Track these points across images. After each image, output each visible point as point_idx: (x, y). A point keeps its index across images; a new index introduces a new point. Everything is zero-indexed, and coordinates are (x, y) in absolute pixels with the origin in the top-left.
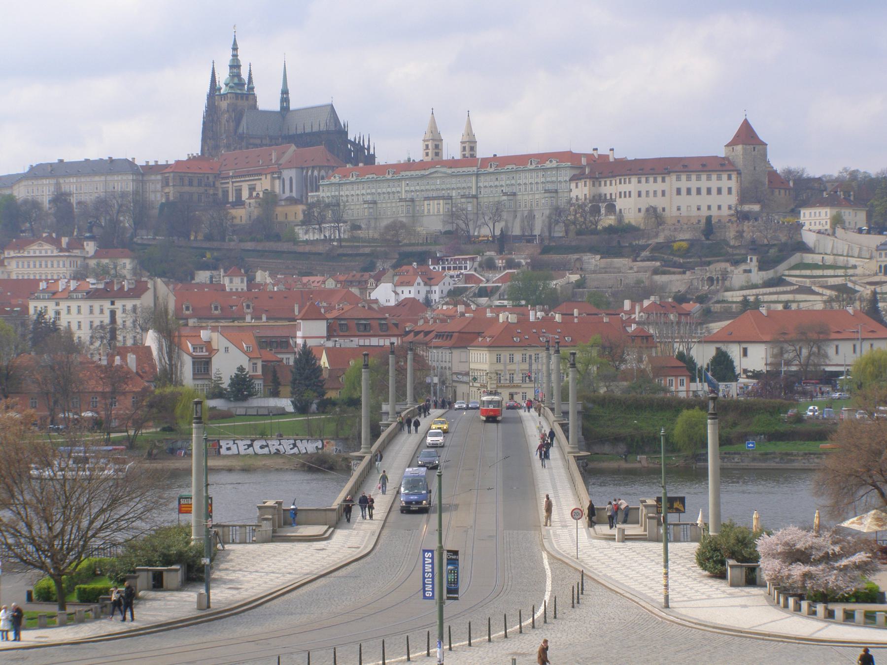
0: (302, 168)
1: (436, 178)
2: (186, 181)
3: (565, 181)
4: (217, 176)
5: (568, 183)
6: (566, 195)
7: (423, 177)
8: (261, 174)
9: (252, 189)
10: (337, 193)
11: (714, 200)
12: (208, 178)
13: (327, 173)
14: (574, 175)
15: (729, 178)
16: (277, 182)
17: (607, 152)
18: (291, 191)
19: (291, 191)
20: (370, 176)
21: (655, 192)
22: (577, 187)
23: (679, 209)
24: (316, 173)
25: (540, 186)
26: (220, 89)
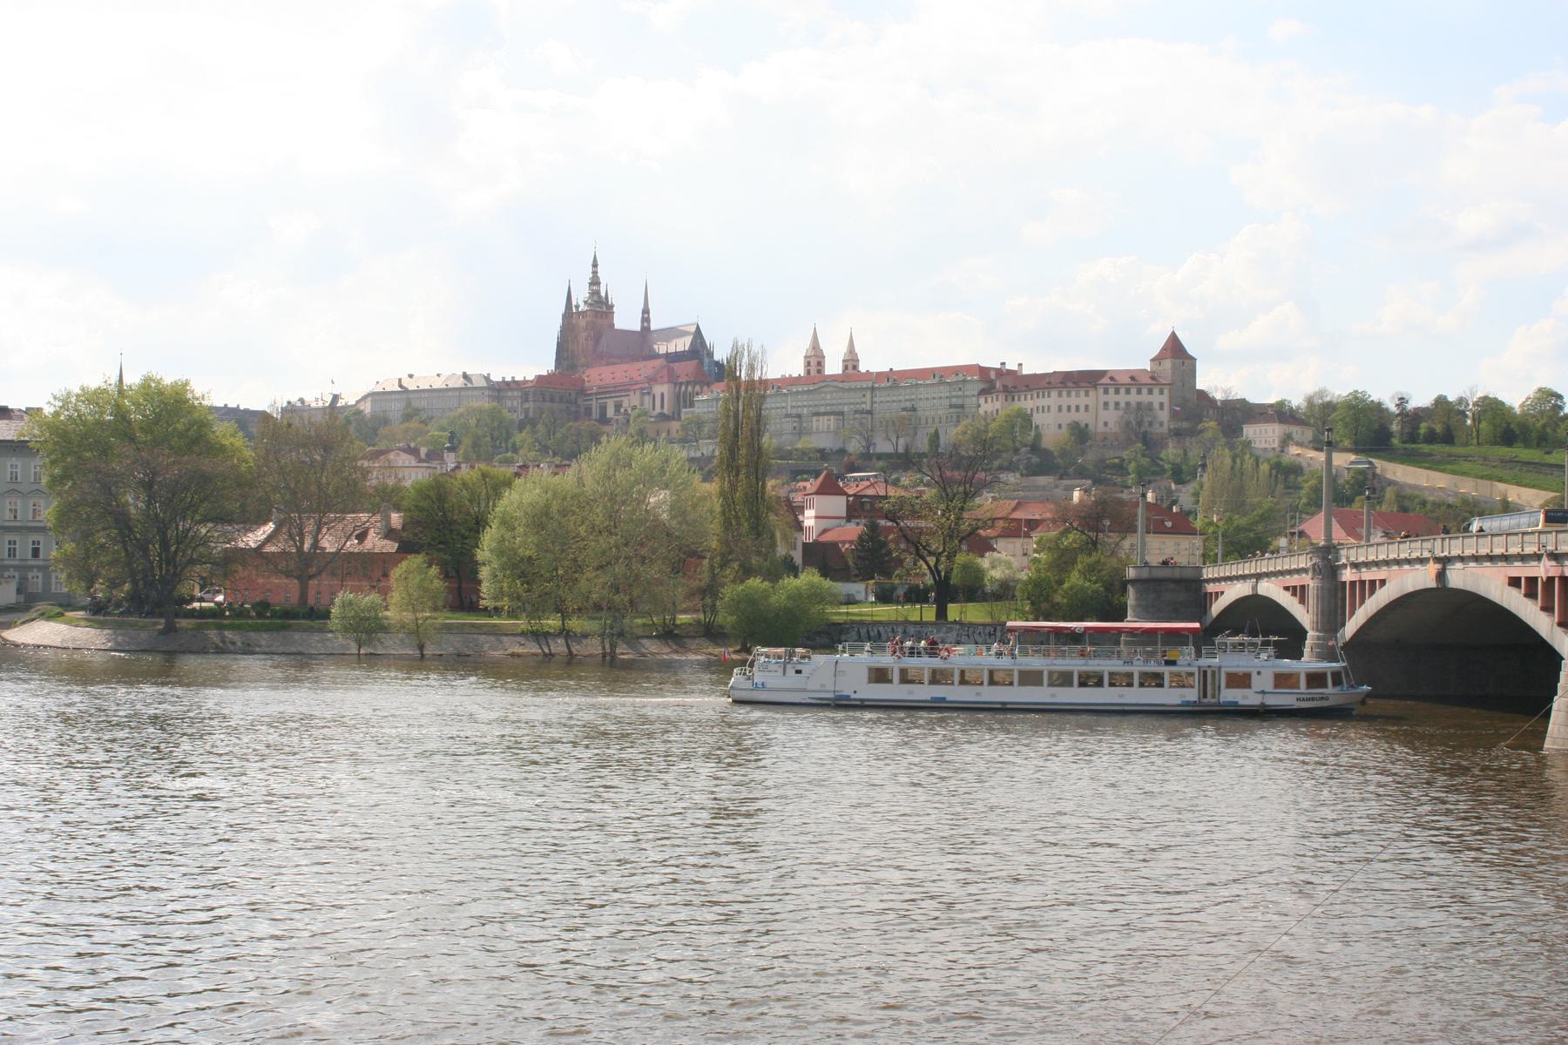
0: (675, 384)
1: (826, 393)
3: (973, 396)
7: (809, 392)
8: (629, 390)
9: (618, 406)
12: (570, 394)
16: (647, 398)
17: (1015, 368)
18: (662, 407)
19: (662, 407)
21: (1077, 408)
22: (986, 402)
24: (690, 389)
25: (947, 402)
26: (577, 307)
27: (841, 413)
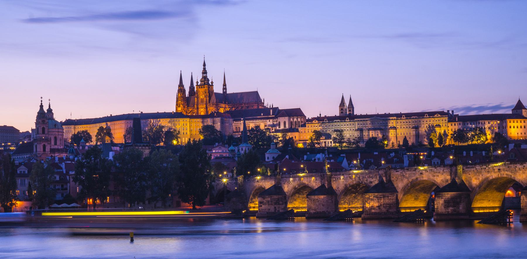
5: (447, 124)
20: (337, 121)
24: (299, 120)
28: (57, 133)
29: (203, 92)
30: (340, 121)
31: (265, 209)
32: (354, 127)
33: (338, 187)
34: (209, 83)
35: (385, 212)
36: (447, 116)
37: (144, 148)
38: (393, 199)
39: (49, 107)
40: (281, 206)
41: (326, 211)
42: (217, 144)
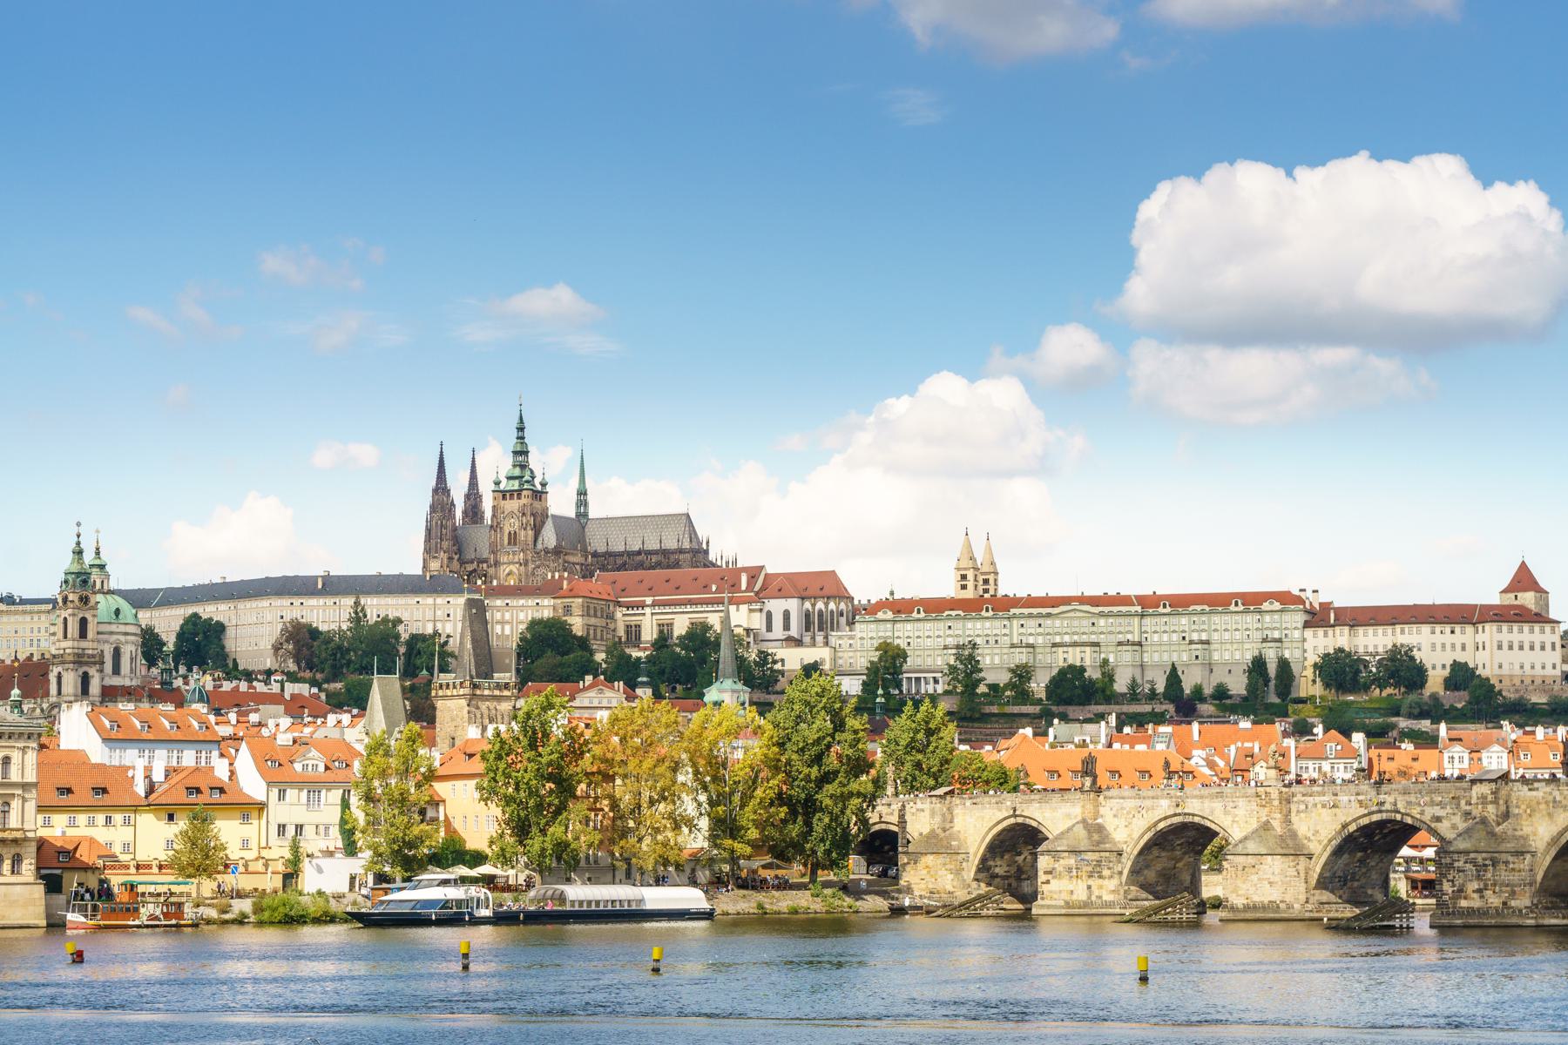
2: (592, 612)
4: (619, 604)
6: (1295, 645)
7: (1049, 615)
10: (890, 634)
11: (1537, 657)
13: (847, 606)
14: (1306, 622)
15: (1553, 631)
16: (757, 615)
18: (787, 627)
19: (787, 627)
20: (953, 613)
21: (1453, 646)
23: (1500, 667)
24: (832, 606)
27: (1097, 644)
28: (122, 638)
29: (516, 511)
30: (962, 614)
31: (1060, 891)
32: (1005, 635)
33: (1318, 832)
34: (534, 486)
35: (1496, 909)
36: (1301, 607)
37: (497, 693)
38: (1520, 871)
39: (98, 553)
40: (1106, 882)
41: (1282, 902)
42: (589, 679)
